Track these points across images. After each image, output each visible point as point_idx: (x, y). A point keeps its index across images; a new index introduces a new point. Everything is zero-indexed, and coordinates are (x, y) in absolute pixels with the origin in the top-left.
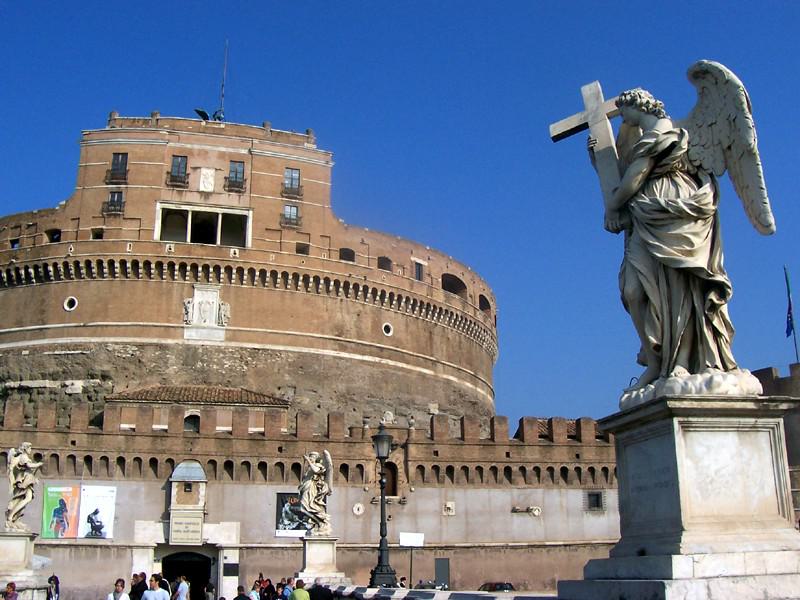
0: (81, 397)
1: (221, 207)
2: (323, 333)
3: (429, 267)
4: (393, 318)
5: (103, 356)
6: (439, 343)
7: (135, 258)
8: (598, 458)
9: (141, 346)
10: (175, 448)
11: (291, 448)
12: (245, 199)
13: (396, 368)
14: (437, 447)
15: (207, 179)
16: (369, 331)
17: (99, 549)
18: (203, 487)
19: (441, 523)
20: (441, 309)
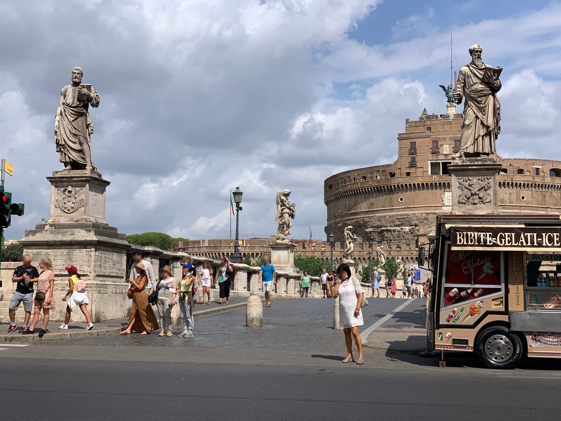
0: (408, 232)
3: (542, 168)
7: (422, 182)
9: (428, 214)
15: (446, 149)
20: (549, 185)
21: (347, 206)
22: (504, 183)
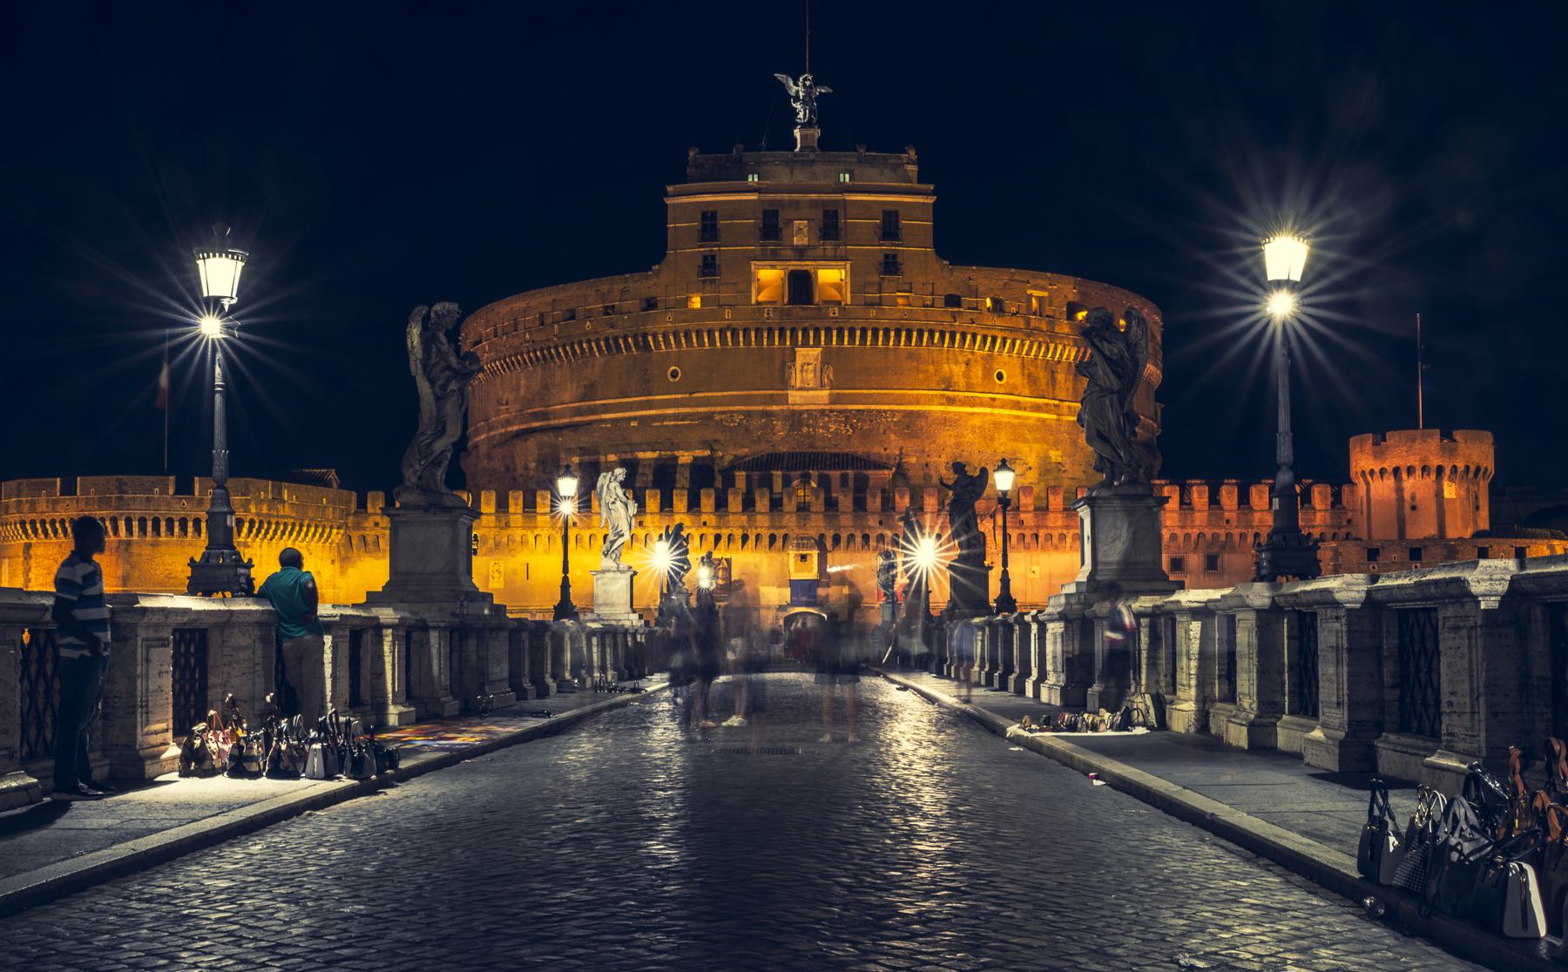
3: (1050, 296)
6: (1063, 381)
9: (748, 414)
13: (1009, 416)
14: (1023, 516)
15: (800, 234)
16: (980, 380)
21: (522, 390)
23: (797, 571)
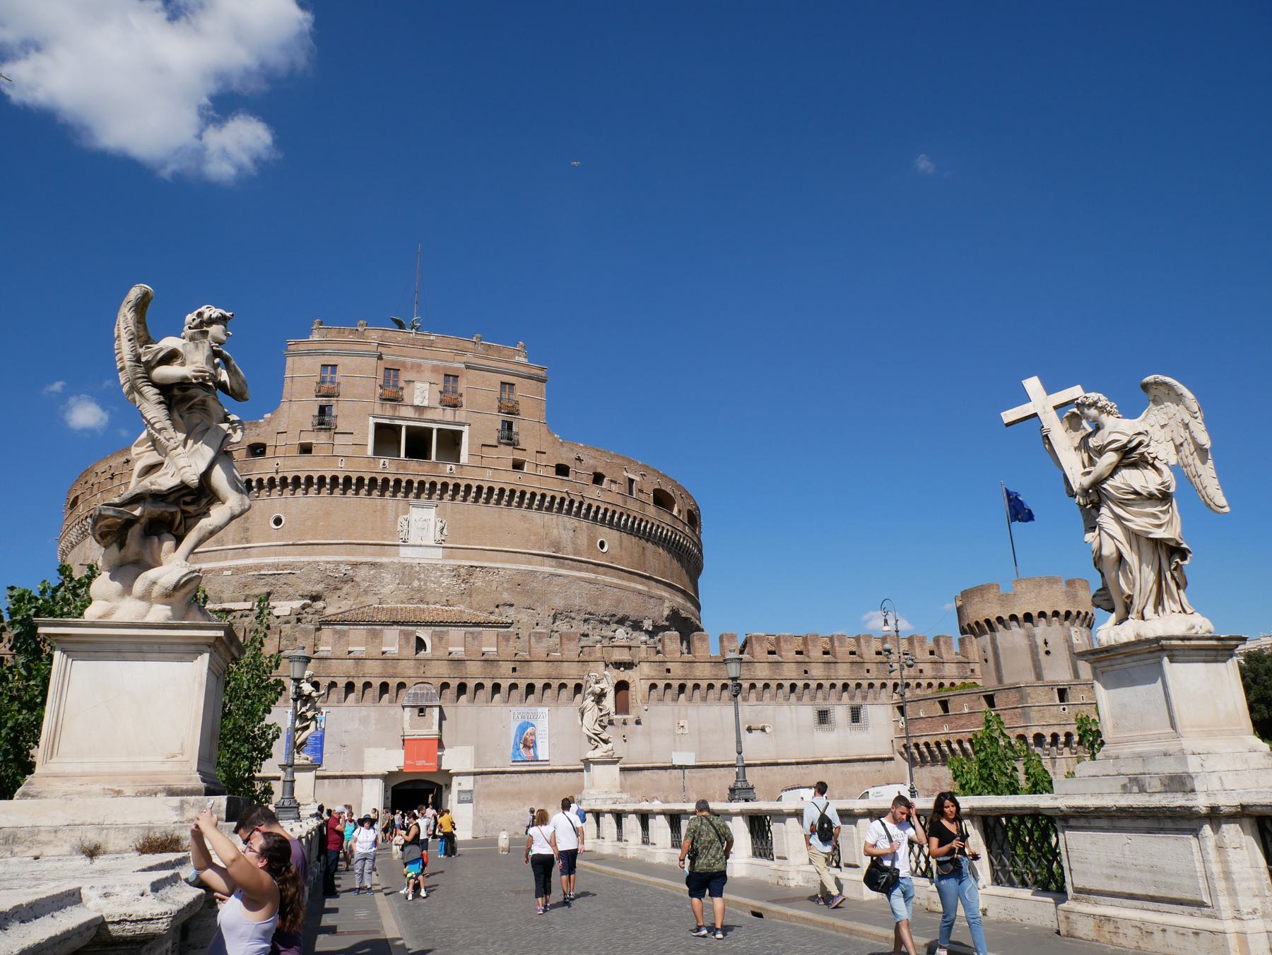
1: (434, 421)
2: (539, 548)
4: (610, 537)
5: (315, 576)
7: (347, 474)
8: (826, 673)
9: (355, 565)
10: (407, 670)
11: (527, 667)
12: (461, 415)
14: (669, 665)
15: (422, 393)
17: (326, 781)
18: (436, 710)
19: (675, 741)
22: (563, 500)
23: (412, 727)
